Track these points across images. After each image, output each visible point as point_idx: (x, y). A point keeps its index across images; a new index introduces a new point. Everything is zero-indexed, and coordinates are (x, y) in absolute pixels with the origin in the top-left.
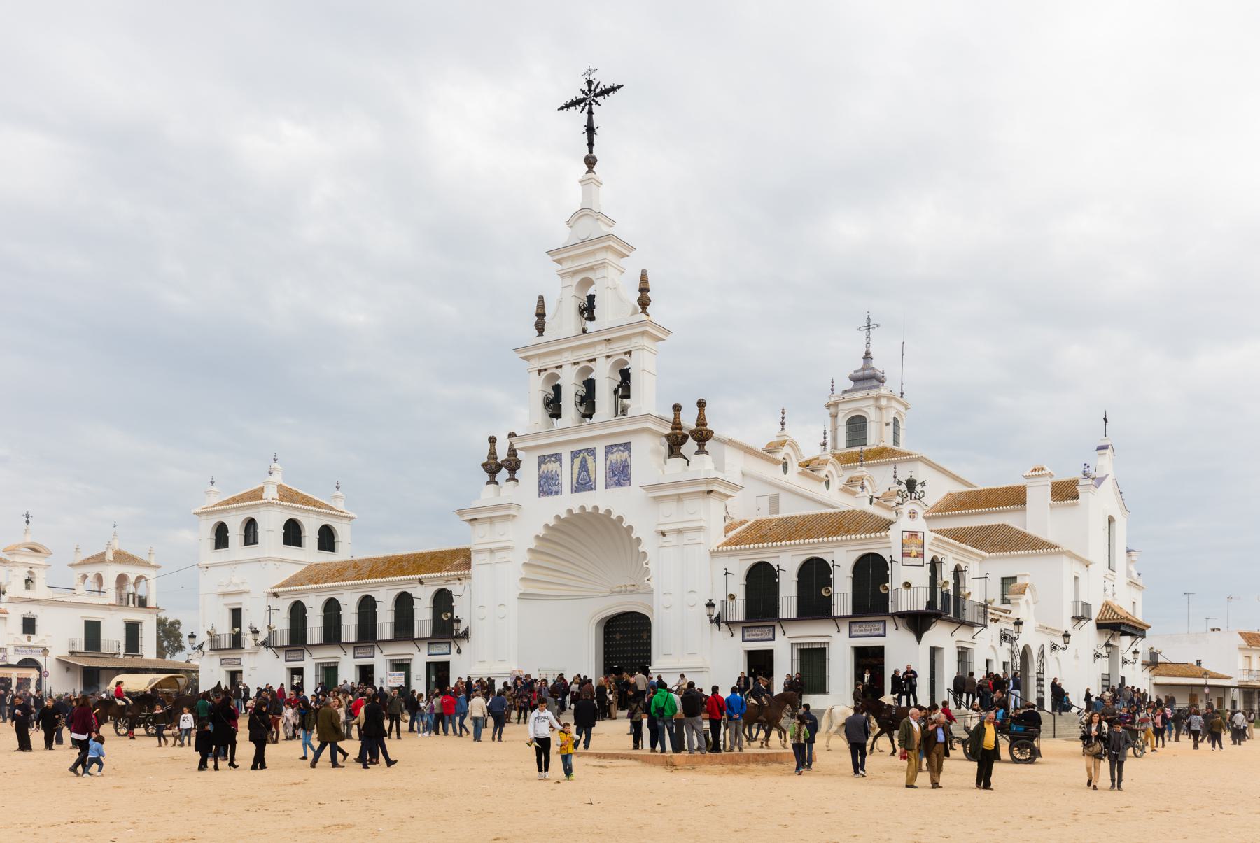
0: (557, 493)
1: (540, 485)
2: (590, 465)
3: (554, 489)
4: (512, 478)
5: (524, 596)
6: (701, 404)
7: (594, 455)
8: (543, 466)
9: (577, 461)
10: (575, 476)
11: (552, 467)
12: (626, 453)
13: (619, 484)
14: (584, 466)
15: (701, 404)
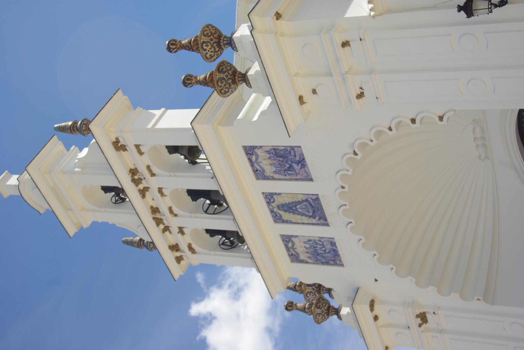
0: (333, 244)
1: (327, 263)
2: (287, 200)
3: (328, 247)
4: (329, 291)
5: (489, 296)
6: (173, 46)
7: (272, 195)
8: (302, 257)
9: (286, 216)
10: (305, 219)
11: (300, 248)
12: (258, 152)
13: (302, 162)
14: (290, 207)
15: (173, 46)
